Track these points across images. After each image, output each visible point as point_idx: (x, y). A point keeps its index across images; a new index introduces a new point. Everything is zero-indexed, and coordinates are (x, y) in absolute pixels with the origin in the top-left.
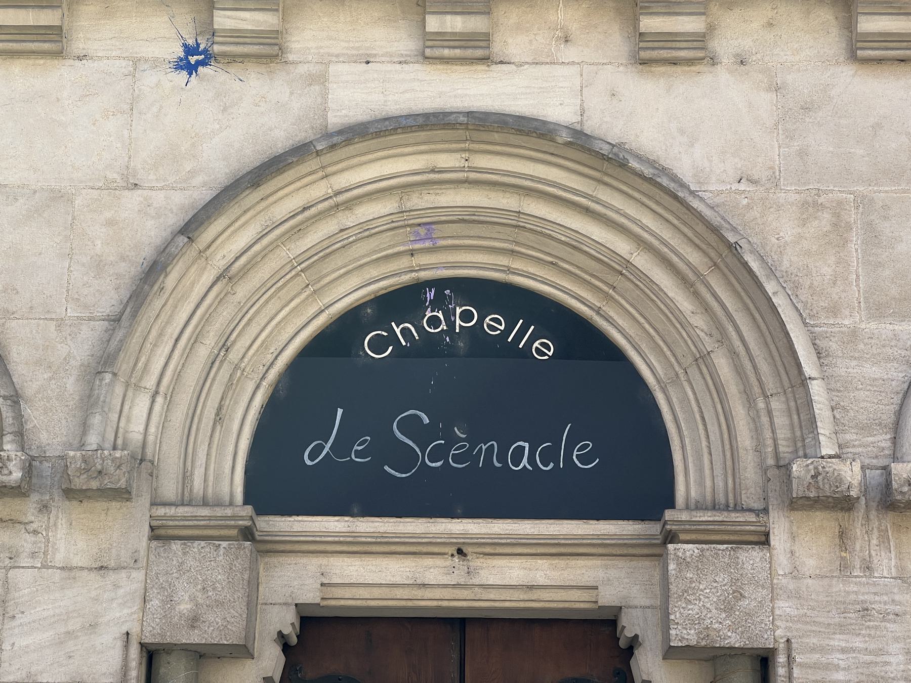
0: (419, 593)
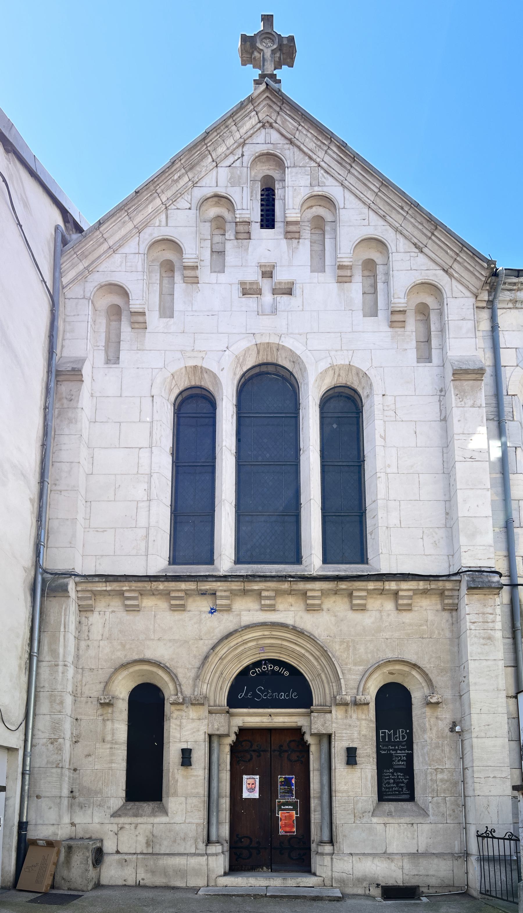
0: (262, 724)
